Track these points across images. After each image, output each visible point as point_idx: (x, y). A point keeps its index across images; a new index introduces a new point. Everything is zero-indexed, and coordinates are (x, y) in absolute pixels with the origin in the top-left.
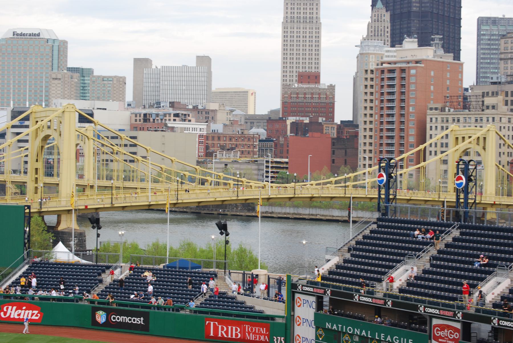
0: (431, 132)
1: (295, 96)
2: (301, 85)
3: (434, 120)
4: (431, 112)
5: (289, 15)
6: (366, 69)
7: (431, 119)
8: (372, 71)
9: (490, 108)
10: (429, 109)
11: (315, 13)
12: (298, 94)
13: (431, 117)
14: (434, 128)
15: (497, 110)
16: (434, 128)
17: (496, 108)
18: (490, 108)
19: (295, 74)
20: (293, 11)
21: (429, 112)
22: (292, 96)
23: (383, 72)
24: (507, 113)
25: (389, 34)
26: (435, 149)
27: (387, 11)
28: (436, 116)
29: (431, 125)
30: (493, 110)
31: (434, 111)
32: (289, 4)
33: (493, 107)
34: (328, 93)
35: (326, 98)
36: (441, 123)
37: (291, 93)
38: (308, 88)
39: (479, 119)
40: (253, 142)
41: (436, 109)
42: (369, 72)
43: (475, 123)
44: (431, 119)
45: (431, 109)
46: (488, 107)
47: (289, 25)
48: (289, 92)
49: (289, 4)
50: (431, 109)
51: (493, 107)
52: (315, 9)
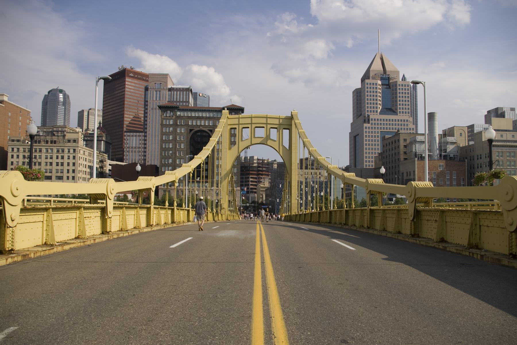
0: (12, 160)
3: (15, 150)
4: (13, 143)
7: (13, 149)
9: (72, 141)
13: (13, 147)
14: (15, 156)
15: (78, 143)
16: (15, 156)
17: (76, 142)
18: (72, 141)
24: (83, 147)
30: (74, 144)
31: (15, 142)
33: (75, 141)
36: (22, 153)
39: (60, 150)
41: (18, 141)
43: (56, 154)
44: (13, 149)
46: (69, 141)
51: (75, 141)
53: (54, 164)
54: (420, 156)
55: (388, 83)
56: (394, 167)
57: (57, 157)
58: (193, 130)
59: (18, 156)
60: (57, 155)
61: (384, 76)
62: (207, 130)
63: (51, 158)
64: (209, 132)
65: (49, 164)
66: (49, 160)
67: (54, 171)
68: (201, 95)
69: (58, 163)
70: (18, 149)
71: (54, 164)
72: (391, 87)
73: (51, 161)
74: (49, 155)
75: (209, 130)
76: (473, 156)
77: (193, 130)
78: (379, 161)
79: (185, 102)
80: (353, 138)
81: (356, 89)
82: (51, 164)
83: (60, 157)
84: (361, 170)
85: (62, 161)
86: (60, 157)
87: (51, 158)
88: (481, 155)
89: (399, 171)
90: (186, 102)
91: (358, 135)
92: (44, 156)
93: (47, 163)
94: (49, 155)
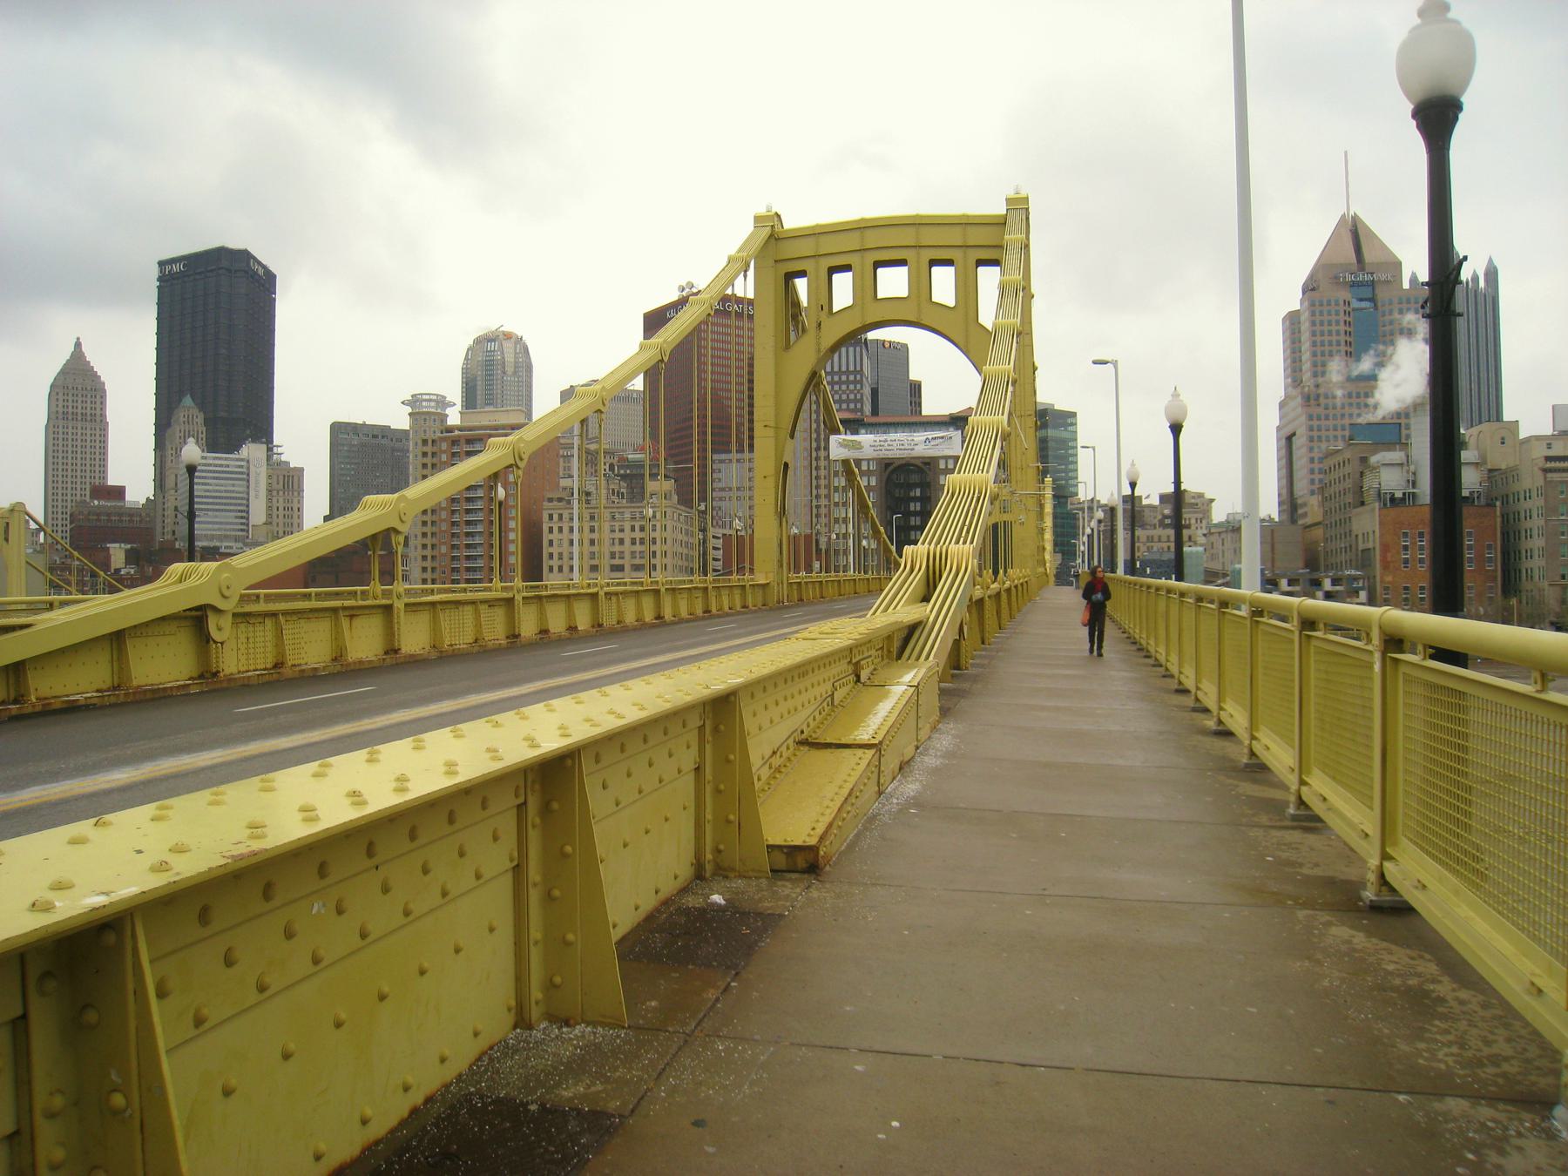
1: (95, 517)
2: (102, 503)
3: (556, 517)
4: (551, 504)
5: (60, 410)
6: (425, 438)
7: (551, 517)
8: (433, 441)
10: (546, 499)
11: (98, 409)
12: (98, 515)
13: (550, 512)
14: (556, 530)
16: (556, 530)
19: (88, 487)
20: (66, 404)
21: (546, 504)
22: (91, 517)
23: (455, 442)
25: (204, 441)
26: (560, 563)
27: (200, 411)
28: (560, 512)
29: (551, 525)
31: (555, 503)
32: (61, 394)
34: (144, 514)
35: (140, 521)
37: (89, 514)
38: (114, 507)
40: (83, 576)
42: (430, 442)
44: (551, 517)
45: (550, 500)
47: (61, 423)
48: (86, 513)
49: (61, 394)
50: (550, 500)
52: (98, 403)
53: (627, 542)
54: (1388, 496)
55: (1371, 296)
56: (1343, 521)
57: (633, 528)
58: (892, 464)
59: (560, 530)
60: (632, 523)
61: (1360, 278)
62: (920, 465)
63: (622, 530)
64: (923, 466)
65: (617, 541)
66: (618, 535)
67: (627, 556)
68: (887, 345)
69: (635, 539)
70: (561, 516)
71: (627, 542)
72: (1379, 304)
73: (621, 535)
74: (617, 525)
75: (922, 463)
76: (1518, 493)
77: (892, 464)
78: (1319, 507)
79: (852, 373)
80: (1284, 440)
81: (1290, 312)
82: (622, 541)
83: (637, 528)
84: (1272, 531)
85: (642, 535)
86: (637, 528)
87: (622, 530)
88: (1530, 490)
89: (1350, 531)
90: (855, 372)
91: (1294, 434)
92: (606, 527)
93: (613, 539)
94: (617, 525)
